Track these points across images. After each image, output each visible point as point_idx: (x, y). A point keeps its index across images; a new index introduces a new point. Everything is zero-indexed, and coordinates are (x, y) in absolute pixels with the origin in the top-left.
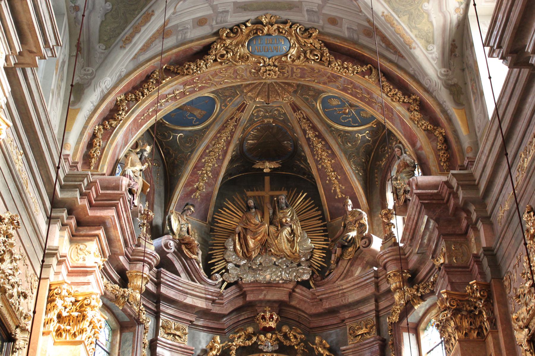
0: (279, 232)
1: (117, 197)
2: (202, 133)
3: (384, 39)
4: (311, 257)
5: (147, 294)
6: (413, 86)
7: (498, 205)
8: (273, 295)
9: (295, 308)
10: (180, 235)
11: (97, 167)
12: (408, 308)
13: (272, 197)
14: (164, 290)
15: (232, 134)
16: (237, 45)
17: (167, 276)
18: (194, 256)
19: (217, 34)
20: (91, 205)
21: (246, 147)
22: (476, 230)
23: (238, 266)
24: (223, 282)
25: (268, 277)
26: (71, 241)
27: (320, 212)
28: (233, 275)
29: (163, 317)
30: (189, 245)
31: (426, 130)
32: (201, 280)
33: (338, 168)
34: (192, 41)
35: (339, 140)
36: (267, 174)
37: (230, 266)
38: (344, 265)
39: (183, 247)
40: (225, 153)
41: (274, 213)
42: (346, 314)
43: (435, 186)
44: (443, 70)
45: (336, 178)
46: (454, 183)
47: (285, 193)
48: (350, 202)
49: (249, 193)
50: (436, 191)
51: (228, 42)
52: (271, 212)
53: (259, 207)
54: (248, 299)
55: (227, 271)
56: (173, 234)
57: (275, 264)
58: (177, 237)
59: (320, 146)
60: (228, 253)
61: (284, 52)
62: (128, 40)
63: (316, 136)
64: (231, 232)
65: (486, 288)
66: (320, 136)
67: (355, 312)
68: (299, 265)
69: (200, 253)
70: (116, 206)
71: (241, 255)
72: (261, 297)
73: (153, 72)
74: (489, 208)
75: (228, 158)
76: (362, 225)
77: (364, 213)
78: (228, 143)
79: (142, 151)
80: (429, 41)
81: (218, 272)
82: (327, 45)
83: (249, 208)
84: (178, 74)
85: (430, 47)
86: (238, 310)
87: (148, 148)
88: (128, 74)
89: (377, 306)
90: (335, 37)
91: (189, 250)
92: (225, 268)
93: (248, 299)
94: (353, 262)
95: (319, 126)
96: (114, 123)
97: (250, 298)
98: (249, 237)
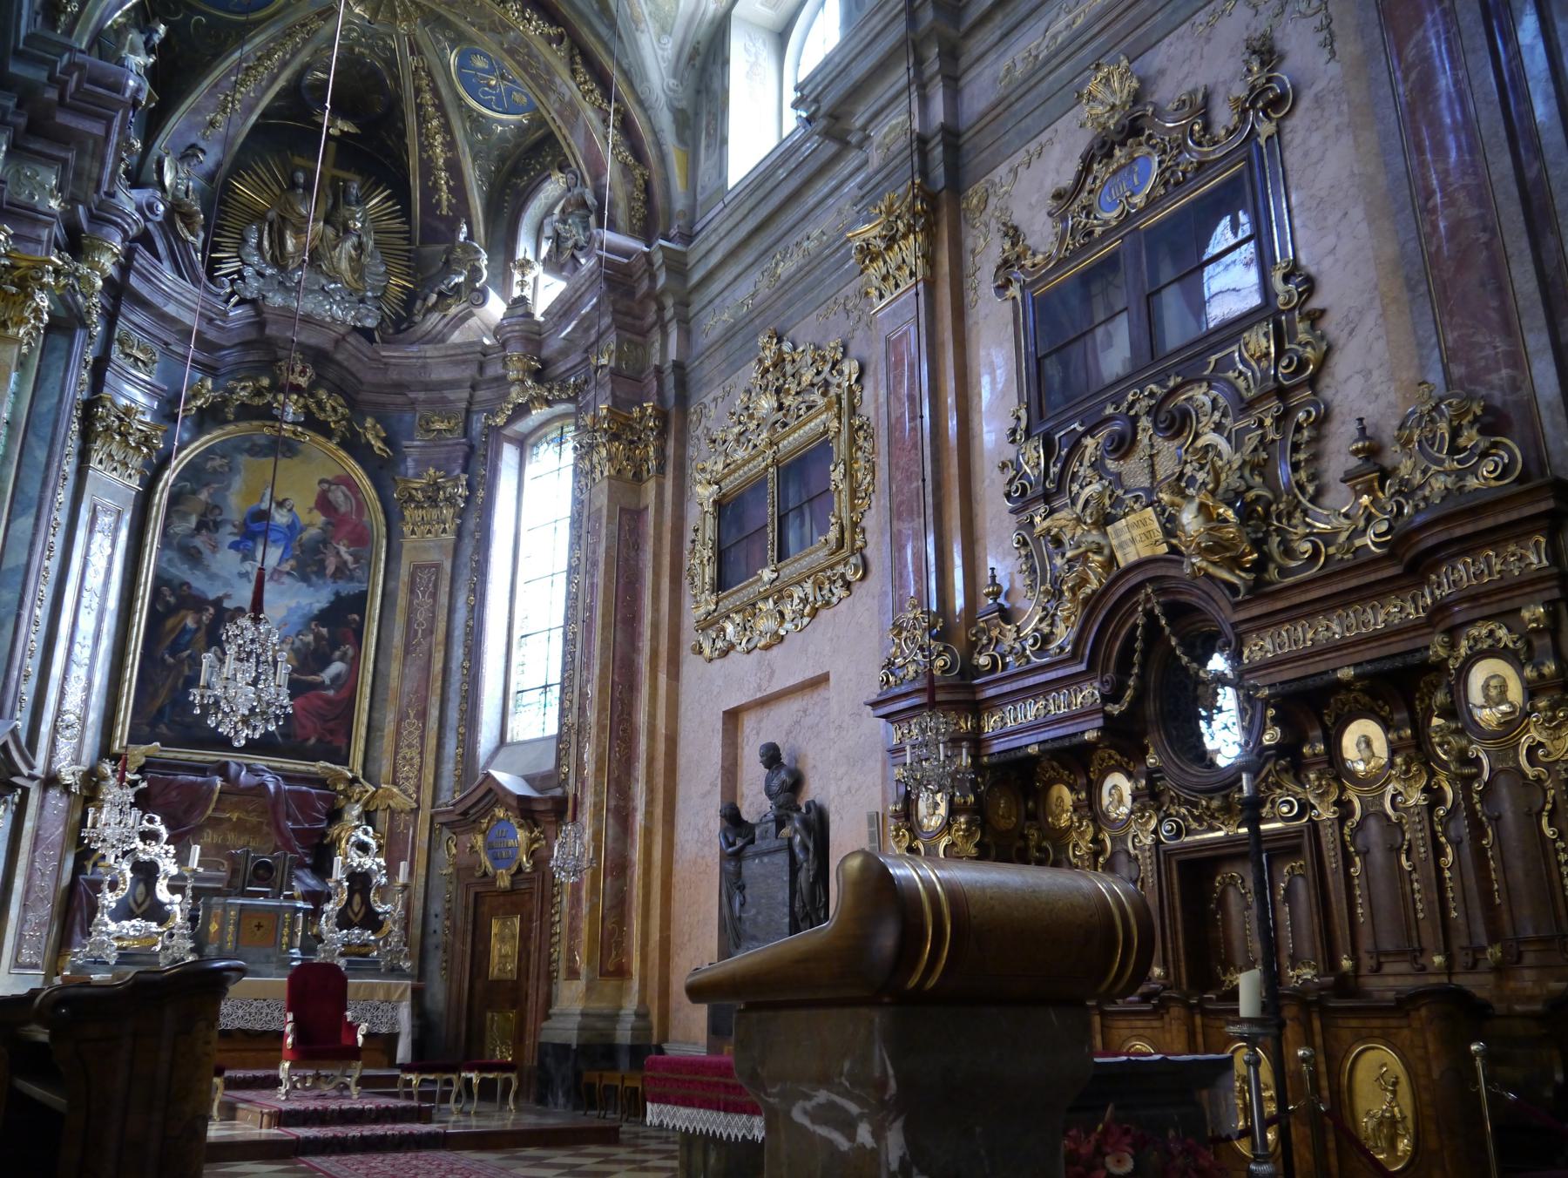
0: (339, 240)
4: (383, 294)
5: (108, 281)
7: (709, 309)
9: (339, 364)
10: (174, 196)
12: (521, 411)
14: (134, 280)
17: (142, 259)
18: (191, 238)
22: (665, 335)
23: (260, 274)
24: (232, 294)
28: (253, 287)
29: (121, 322)
30: (188, 219)
32: (196, 281)
33: (454, 168)
35: (468, 125)
37: (248, 272)
42: (422, 396)
43: (627, 253)
45: (447, 183)
46: (658, 259)
47: (358, 178)
48: (465, 229)
50: (626, 261)
52: (330, 202)
55: (242, 278)
57: (323, 289)
58: (170, 198)
59: (435, 123)
60: (248, 249)
63: (434, 105)
66: (440, 107)
67: (436, 395)
69: (202, 235)
70: (110, 121)
71: (268, 257)
76: (475, 273)
81: (226, 275)
83: (293, 185)
86: (246, 345)
89: (471, 396)
91: (187, 226)
92: (239, 272)
97: (271, 331)
98: (288, 234)
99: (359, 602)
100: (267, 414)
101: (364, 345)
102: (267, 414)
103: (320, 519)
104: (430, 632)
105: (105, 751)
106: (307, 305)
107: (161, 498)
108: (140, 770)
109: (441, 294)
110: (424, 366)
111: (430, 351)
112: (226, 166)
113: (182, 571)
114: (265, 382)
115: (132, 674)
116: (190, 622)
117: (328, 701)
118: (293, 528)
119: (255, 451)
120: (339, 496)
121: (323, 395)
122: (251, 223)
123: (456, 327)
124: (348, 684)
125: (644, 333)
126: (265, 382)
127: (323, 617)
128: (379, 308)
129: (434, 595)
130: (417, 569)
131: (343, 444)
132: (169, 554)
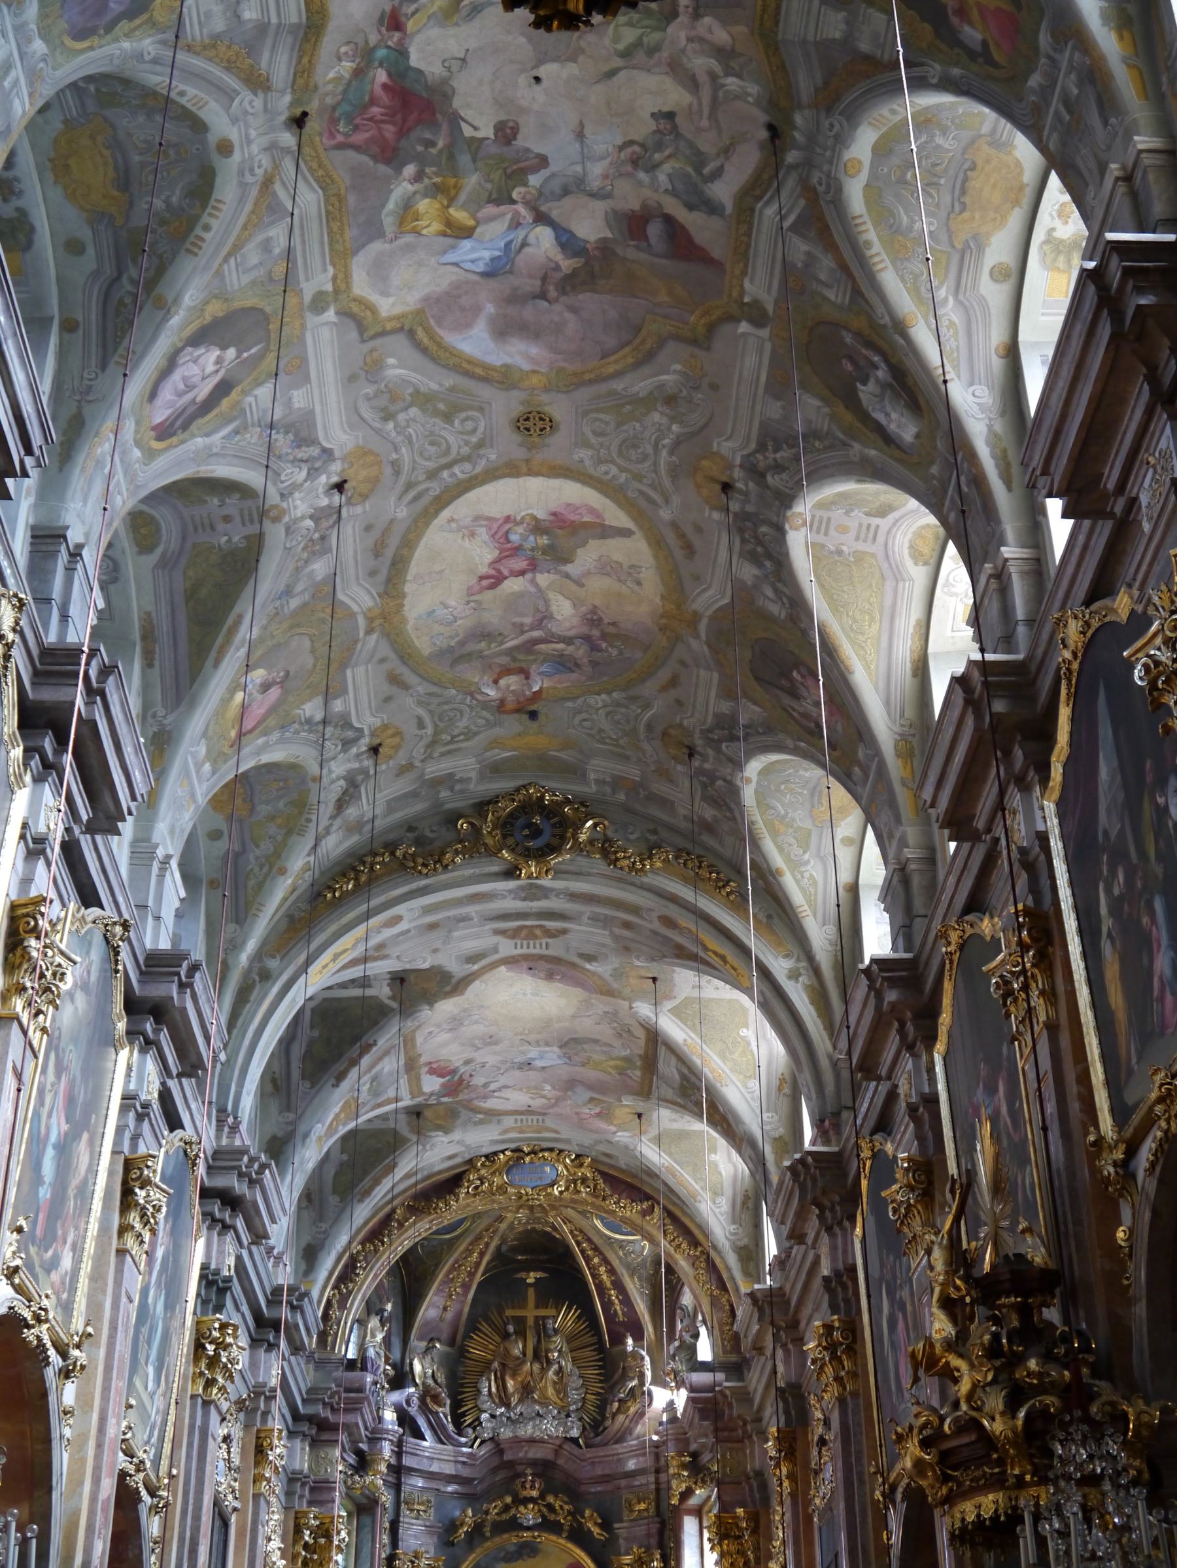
0: (544, 1371)
1: (360, 1401)
2: (451, 1244)
3: (666, 1184)
6: (700, 1237)
8: (535, 1453)
11: (333, 1348)
13: (537, 1318)
14: (407, 1461)
15: (487, 1245)
16: (493, 1173)
19: (471, 1162)
20: (333, 1409)
21: (504, 1248)
22: (752, 1442)
25: (530, 1431)
26: (311, 1446)
27: (595, 1339)
30: (436, 1399)
31: (711, 1295)
34: (440, 1172)
36: (530, 1285)
37: (485, 1416)
39: (428, 1400)
40: (478, 1264)
41: (539, 1341)
43: (711, 1388)
44: (732, 1228)
47: (553, 1312)
49: (509, 1313)
53: (521, 1333)
54: (506, 1458)
56: (416, 1385)
57: (538, 1414)
59: (596, 1260)
61: (549, 1181)
62: (367, 1193)
64: (486, 1366)
66: (596, 1249)
68: (568, 1416)
70: (360, 1409)
72: (521, 1455)
73: (393, 1211)
74: (764, 1422)
76: (642, 1376)
77: (647, 1359)
78: (482, 1254)
79: (382, 1311)
80: (716, 1193)
82: (602, 1173)
84: (422, 1212)
85: (718, 1200)
87: (389, 1307)
90: (611, 1166)
92: (478, 1419)
93: (506, 1458)
95: (596, 1239)
96: (351, 1285)
97: (508, 1456)
101: (576, 1451)
106: (527, 1430)
109: (620, 1401)
110: (619, 1460)
111: (620, 1448)
112: (461, 1330)
122: (481, 1374)
123: (637, 1423)
125: (741, 1441)
128: (581, 1419)
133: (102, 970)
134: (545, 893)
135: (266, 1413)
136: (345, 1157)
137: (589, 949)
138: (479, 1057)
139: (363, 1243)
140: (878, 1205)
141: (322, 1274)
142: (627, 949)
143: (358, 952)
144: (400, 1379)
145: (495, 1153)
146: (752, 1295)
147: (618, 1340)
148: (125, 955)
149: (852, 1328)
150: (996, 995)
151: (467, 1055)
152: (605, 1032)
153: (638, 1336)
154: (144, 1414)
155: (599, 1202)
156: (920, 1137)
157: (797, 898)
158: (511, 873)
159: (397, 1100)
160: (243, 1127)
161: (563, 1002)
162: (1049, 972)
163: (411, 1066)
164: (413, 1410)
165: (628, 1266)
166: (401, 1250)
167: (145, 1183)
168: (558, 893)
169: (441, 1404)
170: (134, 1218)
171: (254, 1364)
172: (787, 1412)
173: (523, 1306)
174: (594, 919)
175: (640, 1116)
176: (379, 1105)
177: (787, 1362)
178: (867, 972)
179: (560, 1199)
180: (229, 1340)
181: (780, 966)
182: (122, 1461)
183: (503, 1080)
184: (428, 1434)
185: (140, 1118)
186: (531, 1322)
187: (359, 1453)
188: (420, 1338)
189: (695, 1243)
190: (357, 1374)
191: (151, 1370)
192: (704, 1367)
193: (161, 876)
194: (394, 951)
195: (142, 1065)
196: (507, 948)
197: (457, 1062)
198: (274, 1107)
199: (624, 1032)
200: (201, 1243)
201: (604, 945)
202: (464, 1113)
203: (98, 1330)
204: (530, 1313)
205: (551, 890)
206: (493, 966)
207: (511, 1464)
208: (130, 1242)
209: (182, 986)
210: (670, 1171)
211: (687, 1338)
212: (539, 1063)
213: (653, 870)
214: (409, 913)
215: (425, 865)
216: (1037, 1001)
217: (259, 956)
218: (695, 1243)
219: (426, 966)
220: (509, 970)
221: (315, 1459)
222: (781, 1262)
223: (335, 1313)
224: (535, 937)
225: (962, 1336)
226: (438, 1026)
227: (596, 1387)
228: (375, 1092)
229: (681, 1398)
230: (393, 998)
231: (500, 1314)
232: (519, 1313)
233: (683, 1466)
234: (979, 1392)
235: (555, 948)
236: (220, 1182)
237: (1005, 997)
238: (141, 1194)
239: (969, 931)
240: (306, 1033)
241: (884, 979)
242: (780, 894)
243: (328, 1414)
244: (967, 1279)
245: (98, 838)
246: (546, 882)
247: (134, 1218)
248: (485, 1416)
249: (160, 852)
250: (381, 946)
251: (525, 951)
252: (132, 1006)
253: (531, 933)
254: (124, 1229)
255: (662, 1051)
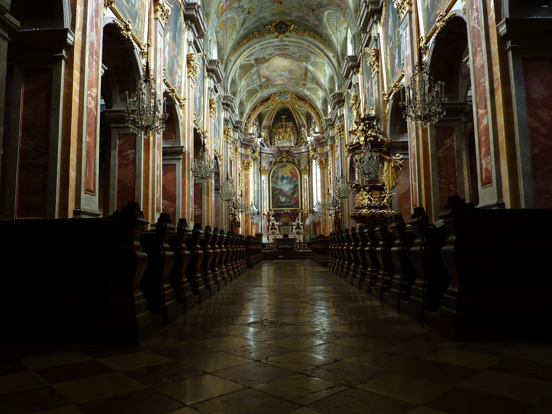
13: (285, 125)
33: (300, 118)
34: (265, 97)
37: (276, 143)
38: (301, 143)
40: (273, 115)
43: (317, 137)
47: (288, 123)
49: (280, 124)
51: (274, 97)
53: (282, 127)
64: (276, 134)
65: (326, 160)
66: (296, 111)
75: (274, 115)
76: (305, 135)
78: (274, 113)
79: (256, 124)
80: (319, 100)
86: (278, 152)
87: (257, 123)
88: (252, 107)
94: (303, 142)
99: (298, 185)
100: (282, 162)
101: (293, 149)
102: (282, 162)
103: (291, 175)
104: (307, 188)
105: (270, 210)
106: (284, 145)
107: (270, 177)
108: (274, 212)
113: (275, 186)
114: (281, 157)
115: (271, 200)
116: (277, 192)
117: (295, 200)
118: (287, 177)
119: (281, 167)
120: (293, 171)
121: (288, 157)
124: (297, 197)
126: (281, 157)
127: (293, 188)
129: (307, 183)
130: (304, 180)
131: (292, 164)
132: (273, 184)
133: (202, 64)
134: (284, 41)
135: (237, 143)
136: (247, 95)
137: (293, 52)
138: (273, 74)
139: (252, 111)
140: (348, 103)
141: (244, 118)
142: (301, 52)
143: (248, 54)
144: (260, 136)
145: (276, 93)
146: (325, 120)
147: (300, 128)
148: (206, 61)
149: (343, 126)
150: (368, 65)
151: (270, 74)
152: (297, 68)
153: (304, 126)
154: (217, 144)
155: (296, 102)
156: (356, 91)
157: (335, 41)
158: (277, 37)
159: (257, 83)
160: (229, 91)
161: (288, 63)
162: (378, 62)
163: (259, 77)
164: (263, 142)
165: (302, 114)
166: (259, 113)
167: (214, 104)
168: (287, 41)
169: (268, 141)
170: (212, 110)
171: (234, 135)
172: (331, 141)
173: (282, 122)
174: (294, 46)
175: (304, 85)
176: (254, 85)
177: (331, 132)
178: (347, 59)
179: (289, 102)
180: (230, 131)
181: (331, 55)
182: (214, 152)
183: (277, 79)
184: (266, 146)
185: (211, 91)
186: (284, 125)
187: (253, 150)
188: (263, 129)
189: (315, 109)
190: (252, 136)
191: (217, 137)
192: (317, 133)
193: (210, 44)
194: (255, 54)
195: (210, 81)
196: (277, 52)
197: (268, 75)
198: (233, 86)
199: (301, 68)
200: (223, 113)
201: (297, 51)
202: (270, 86)
203: (208, 130)
204: (284, 124)
205: (285, 40)
206: (274, 56)
207: (281, 151)
208: (212, 114)
209: (216, 66)
210: (310, 95)
211: (313, 128)
212: (284, 75)
213: (306, 36)
214: (257, 46)
215: (260, 36)
216: (375, 67)
217: (228, 57)
218: (315, 109)
219: (261, 57)
220: (278, 57)
221: (245, 151)
222: (331, 113)
223: (247, 125)
224: (283, 50)
225: (358, 129)
226: (264, 68)
227: (296, 137)
228: (252, 82)
229: (312, 138)
230: (255, 63)
231: (278, 123)
232: (282, 124)
233: (313, 151)
234: (360, 138)
235: (287, 52)
236: (225, 102)
237: (370, 66)
238: (213, 106)
239: (366, 51)
240: (238, 71)
241: (350, 60)
242: (331, 40)
243: (247, 143)
244: (360, 118)
245: (199, 39)
246: (284, 39)
247: (212, 110)
248: (276, 143)
249: (209, 39)
250: (252, 53)
251: (281, 53)
252: (208, 70)
253: (282, 49)
254: (211, 112)
255: (308, 72)
